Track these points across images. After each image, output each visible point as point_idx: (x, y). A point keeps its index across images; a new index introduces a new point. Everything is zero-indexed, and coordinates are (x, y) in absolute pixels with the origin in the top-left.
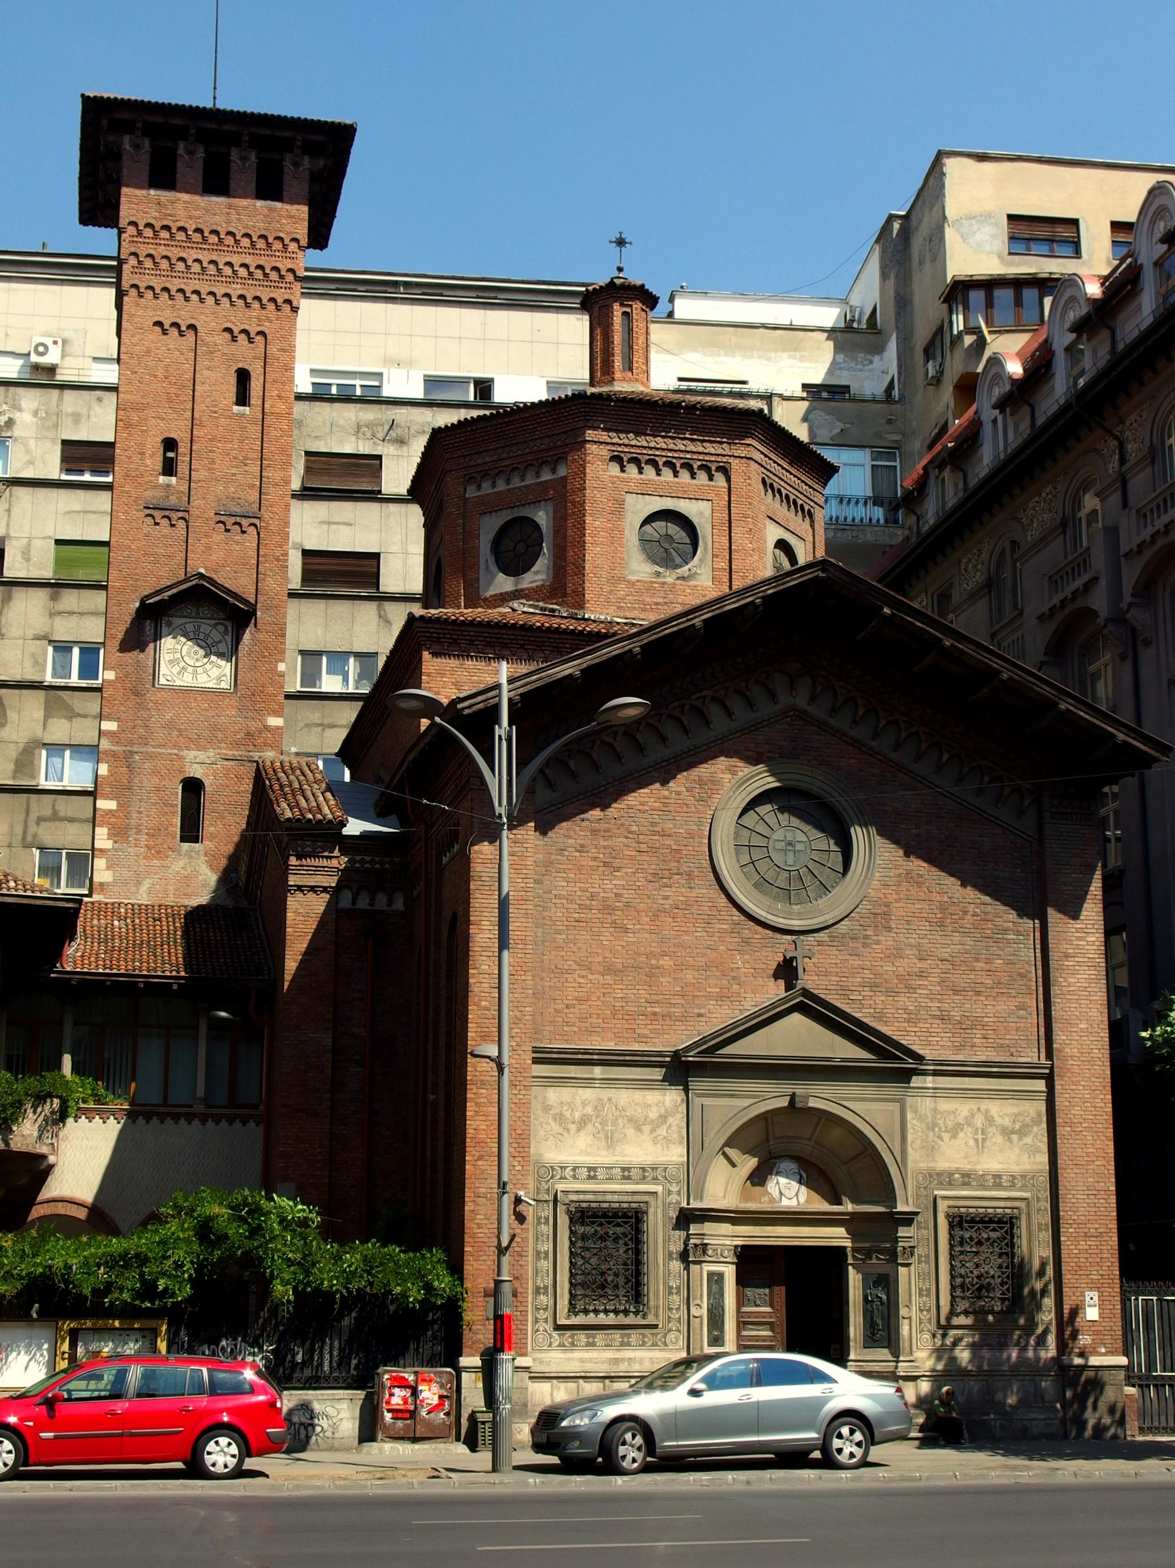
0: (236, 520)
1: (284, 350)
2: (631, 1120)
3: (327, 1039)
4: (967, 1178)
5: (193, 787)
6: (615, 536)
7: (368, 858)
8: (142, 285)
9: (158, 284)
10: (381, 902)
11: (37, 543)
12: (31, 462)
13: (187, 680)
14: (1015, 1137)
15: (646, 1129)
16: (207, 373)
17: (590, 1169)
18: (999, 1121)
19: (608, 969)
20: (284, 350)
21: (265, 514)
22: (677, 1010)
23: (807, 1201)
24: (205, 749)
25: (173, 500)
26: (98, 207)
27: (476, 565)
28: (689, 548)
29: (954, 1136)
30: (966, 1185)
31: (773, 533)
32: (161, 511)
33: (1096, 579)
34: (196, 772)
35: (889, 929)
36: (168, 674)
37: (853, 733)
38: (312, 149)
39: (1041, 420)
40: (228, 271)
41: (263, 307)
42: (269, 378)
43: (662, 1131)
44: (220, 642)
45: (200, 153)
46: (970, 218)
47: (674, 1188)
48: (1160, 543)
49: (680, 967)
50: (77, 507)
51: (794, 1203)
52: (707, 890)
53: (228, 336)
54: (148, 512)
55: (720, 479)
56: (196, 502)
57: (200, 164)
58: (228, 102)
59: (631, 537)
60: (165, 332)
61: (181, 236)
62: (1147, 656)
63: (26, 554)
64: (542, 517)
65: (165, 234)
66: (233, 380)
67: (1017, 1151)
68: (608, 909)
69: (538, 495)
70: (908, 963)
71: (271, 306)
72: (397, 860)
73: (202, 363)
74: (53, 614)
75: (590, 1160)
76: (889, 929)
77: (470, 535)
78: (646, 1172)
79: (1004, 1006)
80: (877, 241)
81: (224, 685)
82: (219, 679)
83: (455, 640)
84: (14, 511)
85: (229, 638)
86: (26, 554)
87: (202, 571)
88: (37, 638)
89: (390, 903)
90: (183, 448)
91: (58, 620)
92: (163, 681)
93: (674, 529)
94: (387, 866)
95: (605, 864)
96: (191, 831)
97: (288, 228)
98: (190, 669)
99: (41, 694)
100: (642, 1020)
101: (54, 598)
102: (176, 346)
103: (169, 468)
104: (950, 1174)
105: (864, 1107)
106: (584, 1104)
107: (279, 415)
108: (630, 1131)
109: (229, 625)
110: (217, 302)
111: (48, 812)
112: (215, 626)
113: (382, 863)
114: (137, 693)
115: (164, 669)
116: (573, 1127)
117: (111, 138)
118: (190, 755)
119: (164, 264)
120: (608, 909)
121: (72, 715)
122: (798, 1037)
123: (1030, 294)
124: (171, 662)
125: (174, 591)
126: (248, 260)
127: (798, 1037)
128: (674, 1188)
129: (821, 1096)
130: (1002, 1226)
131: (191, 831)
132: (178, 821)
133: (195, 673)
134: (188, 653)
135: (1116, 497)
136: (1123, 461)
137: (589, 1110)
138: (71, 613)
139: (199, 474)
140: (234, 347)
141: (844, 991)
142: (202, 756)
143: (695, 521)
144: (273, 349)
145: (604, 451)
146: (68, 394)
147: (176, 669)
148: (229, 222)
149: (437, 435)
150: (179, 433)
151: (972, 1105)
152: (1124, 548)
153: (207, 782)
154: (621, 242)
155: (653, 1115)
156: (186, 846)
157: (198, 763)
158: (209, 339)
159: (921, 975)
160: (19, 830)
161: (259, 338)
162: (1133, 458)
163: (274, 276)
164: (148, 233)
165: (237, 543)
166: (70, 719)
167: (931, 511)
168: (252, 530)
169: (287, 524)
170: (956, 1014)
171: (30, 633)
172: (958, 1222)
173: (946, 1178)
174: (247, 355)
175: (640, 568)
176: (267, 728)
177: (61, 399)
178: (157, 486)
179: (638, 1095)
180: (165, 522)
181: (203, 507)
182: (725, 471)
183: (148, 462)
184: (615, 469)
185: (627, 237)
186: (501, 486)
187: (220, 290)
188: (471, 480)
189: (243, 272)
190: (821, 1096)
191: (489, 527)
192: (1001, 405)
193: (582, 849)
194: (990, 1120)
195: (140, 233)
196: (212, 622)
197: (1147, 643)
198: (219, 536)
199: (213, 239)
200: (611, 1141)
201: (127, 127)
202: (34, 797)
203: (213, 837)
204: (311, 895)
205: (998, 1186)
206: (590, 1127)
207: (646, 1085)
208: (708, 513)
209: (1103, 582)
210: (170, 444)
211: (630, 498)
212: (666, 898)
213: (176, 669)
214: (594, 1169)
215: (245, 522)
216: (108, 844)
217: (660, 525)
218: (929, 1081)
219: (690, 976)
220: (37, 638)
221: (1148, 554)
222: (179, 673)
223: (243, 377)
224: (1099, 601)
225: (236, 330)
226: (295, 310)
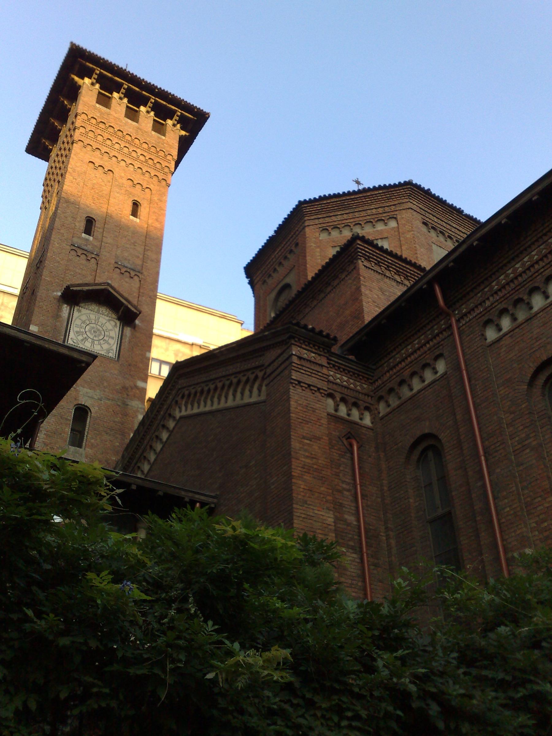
7: (345, 378)
9: (95, 145)
21: (144, 271)
25: (89, 248)
44: (111, 330)
54: (74, 248)
72: (365, 386)
81: (110, 355)
82: (108, 351)
83: (379, 262)
85: (117, 330)
87: (110, 282)
92: (70, 342)
94: (358, 388)
98: (90, 340)
109: (118, 323)
112: (109, 320)
115: (72, 335)
124: (77, 332)
125: (90, 288)
126: (145, 154)
132: (68, 430)
133: (93, 342)
134: (90, 331)
147: (80, 338)
156: (72, 448)
165: (127, 282)
168: (136, 277)
176: (136, 387)
178: (80, 238)
180: (83, 257)
183: (77, 224)
196: (108, 318)
203: (92, 446)
204: (308, 393)
211: (434, 247)
213: (80, 338)
215: (133, 273)
222: (82, 340)
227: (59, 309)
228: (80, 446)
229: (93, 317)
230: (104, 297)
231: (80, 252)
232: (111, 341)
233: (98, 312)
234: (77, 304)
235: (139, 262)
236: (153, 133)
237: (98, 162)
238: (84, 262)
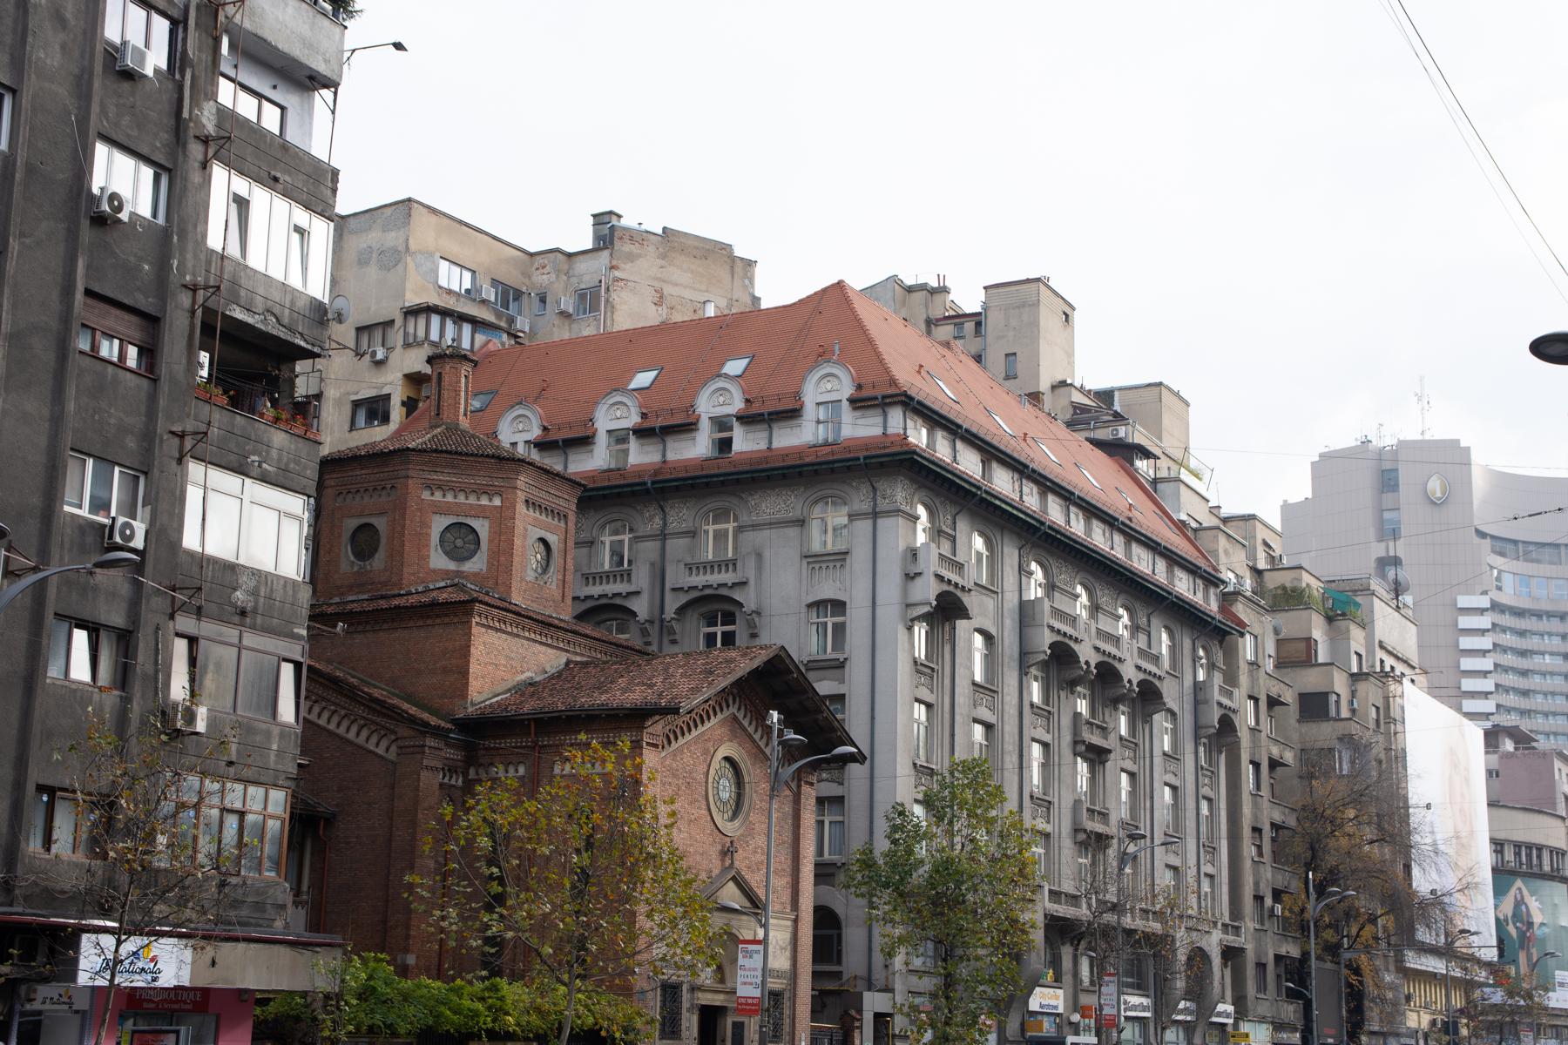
27: (427, 546)
46: (420, 252)
48: (708, 592)
64: (482, 527)
69: (481, 513)
77: (426, 525)
123: (467, 329)
188: (429, 487)
191: (439, 524)
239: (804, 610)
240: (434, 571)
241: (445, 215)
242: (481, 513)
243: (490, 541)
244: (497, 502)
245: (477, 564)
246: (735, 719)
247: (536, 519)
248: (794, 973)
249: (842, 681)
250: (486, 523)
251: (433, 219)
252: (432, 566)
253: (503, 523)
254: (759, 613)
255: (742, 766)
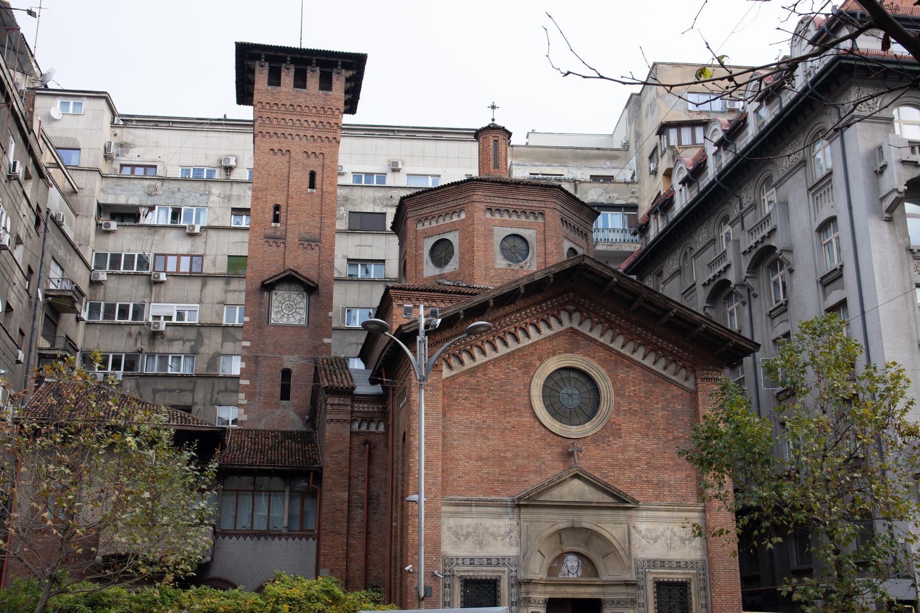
0: (309, 242)
1: (332, 162)
2: (491, 534)
3: (345, 496)
4: (663, 563)
5: (286, 373)
6: (487, 247)
8: (264, 132)
9: (272, 131)
10: (373, 428)
11: (219, 258)
12: (217, 219)
13: (284, 321)
14: (687, 542)
15: (499, 538)
16: (295, 173)
17: (471, 559)
18: (678, 534)
19: (480, 458)
20: (332, 162)
22: (514, 479)
23: (581, 576)
24: (293, 354)
25: (278, 234)
26: (244, 95)
27: (422, 262)
28: (524, 253)
29: (655, 542)
30: (663, 567)
31: (567, 245)
32: (273, 239)
33: (729, 266)
34: (288, 365)
35: (621, 437)
36: (275, 318)
37: (601, 340)
38: (346, 67)
39: (701, 189)
40: (305, 124)
41: (322, 141)
42: (325, 175)
43: (507, 540)
45: (293, 70)
47: (514, 569)
49: (516, 456)
50: (239, 240)
51: (575, 576)
52: (527, 419)
53: (305, 155)
55: (540, 220)
56: (290, 235)
57: (292, 73)
58: (307, 45)
59: (497, 248)
60: (275, 154)
61: (283, 108)
62: (755, 303)
63: (214, 263)
64: (454, 238)
65: (275, 108)
66: (308, 177)
67: (688, 548)
68: (479, 428)
69: (452, 228)
70: (631, 454)
71: (326, 141)
73: (293, 168)
74: (226, 292)
75: (471, 555)
76: (621, 437)
77: (419, 248)
78: (500, 561)
79: (680, 475)
80: (626, 106)
82: (300, 320)
84: (208, 242)
86: (214, 263)
88: (219, 303)
89: (377, 427)
90: (283, 209)
91: (229, 294)
92: (272, 322)
93: (518, 242)
95: (478, 406)
96: (285, 394)
97: (335, 104)
99: (220, 331)
100: (496, 484)
101: (227, 283)
102: (279, 162)
103: (276, 219)
104: (654, 561)
105: (610, 526)
106: (468, 526)
107: (330, 193)
108: (491, 540)
109: (305, 293)
110: (300, 139)
111: (223, 388)
113: (373, 408)
114: (260, 328)
115: (273, 316)
116: (462, 538)
117: (250, 63)
118: (285, 357)
119: (275, 122)
120: (479, 428)
121: (235, 340)
122: (575, 490)
127: (575, 490)
128: (514, 569)
129: (587, 520)
130: (683, 586)
131: (285, 394)
133: (288, 317)
135: (738, 226)
136: (741, 208)
137: (470, 529)
138: (235, 291)
139: (292, 221)
140: (307, 162)
141: (598, 469)
142: (291, 358)
143: (528, 239)
144: (327, 162)
145: (483, 207)
146: (235, 185)
147: (279, 316)
148: (306, 101)
149: (403, 199)
150: (281, 201)
151: (665, 526)
152: (742, 250)
153: (294, 370)
154: (493, 107)
155: (502, 532)
156: (284, 402)
157: (289, 361)
158: (296, 157)
159: (638, 459)
160: (209, 397)
161: (321, 156)
162: (746, 207)
163: (328, 126)
164: (267, 107)
166: (234, 342)
167: (652, 234)
168: (317, 248)
169: (333, 245)
170: (655, 480)
171: (215, 301)
172: (660, 585)
173: (653, 563)
174: (314, 164)
175: (501, 263)
176: (323, 344)
177: (231, 189)
179: (495, 522)
180: (274, 245)
181: (292, 238)
182: (542, 214)
184: (488, 215)
185: (496, 104)
186: (434, 224)
187: (302, 134)
189: (313, 125)
190: (587, 520)
191: (428, 243)
192: (683, 183)
193: (466, 399)
194: (674, 534)
195: (263, 107)
197: (755, 296)
198: (301, 252)
199: (299, 109)
200: (481, 544)
201: (257, 58)
202: (216, 381)
204: (338, 424)
205: (679, 567)
206: (470, 538)
207: (499, 516)
208: (534, 235)
209: (733, 266)
210: (277, 208)
211: (496, 229)
212: (509, 422)
213: (279, 316)
214: (473, 559)
215: (313, 244)
216: (245, 402)
217: (511, 240)
218: (644, 513)
219: (520, 461)
220: (219, 303)
221: (754, 252)
223: (313, 175)
224: (731, 276)
225: (309, 153)
226: (338, 142)
227: (262, 297)
228: (288, 399)
229: (286, 295)
230: (291, 279)
231: (271, 241)
232: (302, 312)
233: (290, 290)
234: (274, 289)
235: (317, 231)
236: (321, 92)
237: (276, 147)
238: (275, 249)
239: (815, 235)
240: (426, 279)
241: (687, 65)
242: (452, 228)
243: (460, 246)
244: (463, 216)
245: (452, 266)
246: (573, 331)
247: (503, 221)
248: (707, 565)
249: (843, 288)
250: (457, 234)
251: (678, 70)
252: (425, 276)
253: (466, 230)
254: (790, 251)
255: (593, 373)
